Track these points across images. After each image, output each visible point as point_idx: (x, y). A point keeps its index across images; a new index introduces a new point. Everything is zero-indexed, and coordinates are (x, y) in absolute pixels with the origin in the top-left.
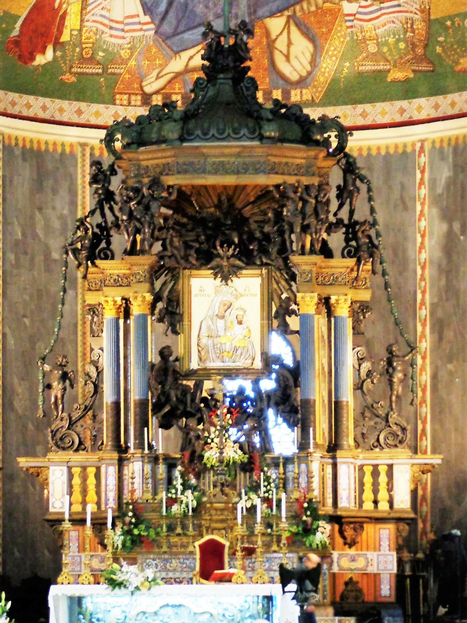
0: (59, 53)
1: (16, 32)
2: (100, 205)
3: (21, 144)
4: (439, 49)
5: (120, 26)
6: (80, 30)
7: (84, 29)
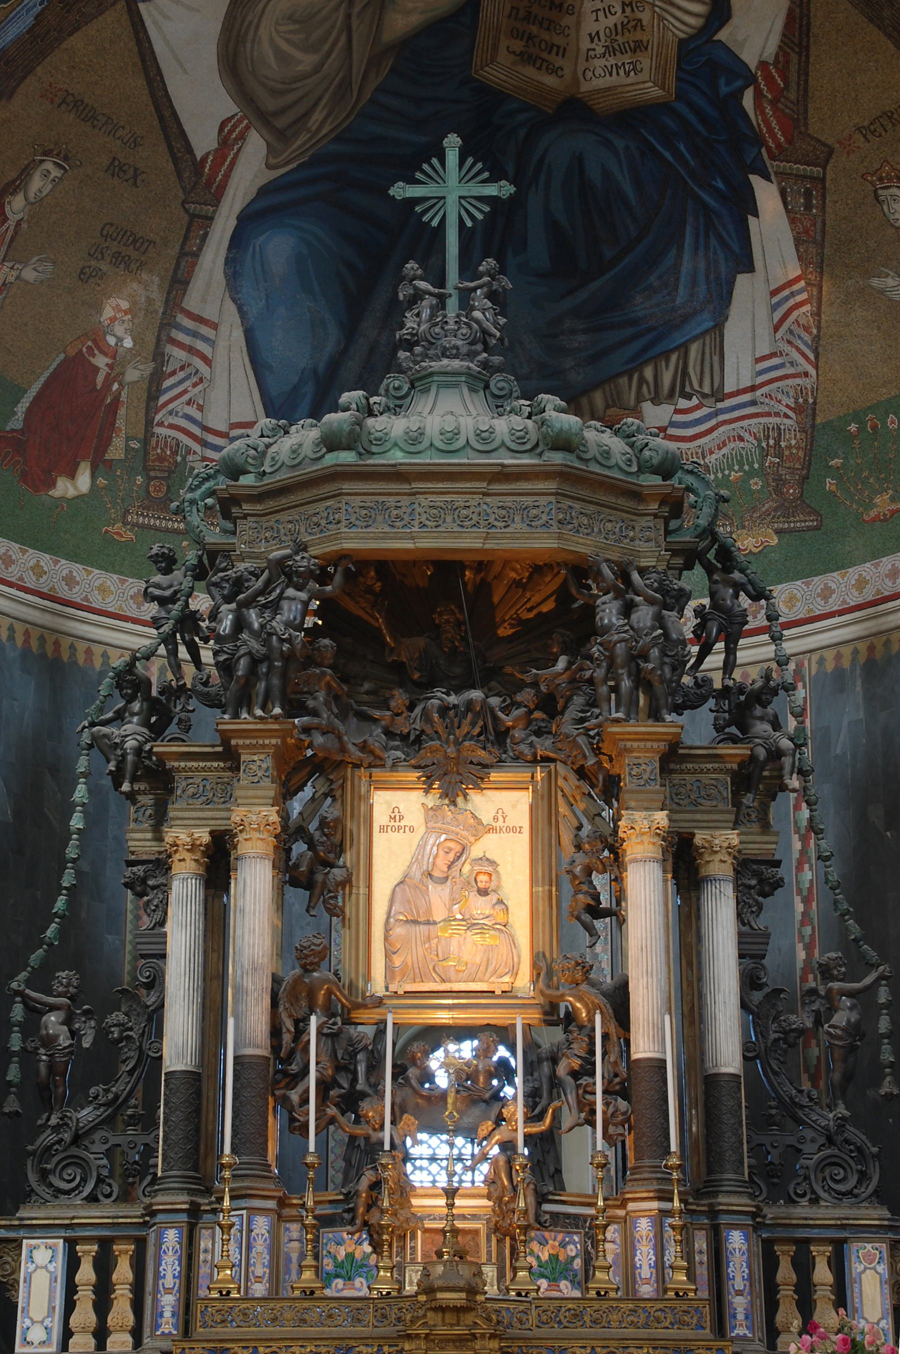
0: (101, 481)
6: (146, 442)
7: (153, 442)
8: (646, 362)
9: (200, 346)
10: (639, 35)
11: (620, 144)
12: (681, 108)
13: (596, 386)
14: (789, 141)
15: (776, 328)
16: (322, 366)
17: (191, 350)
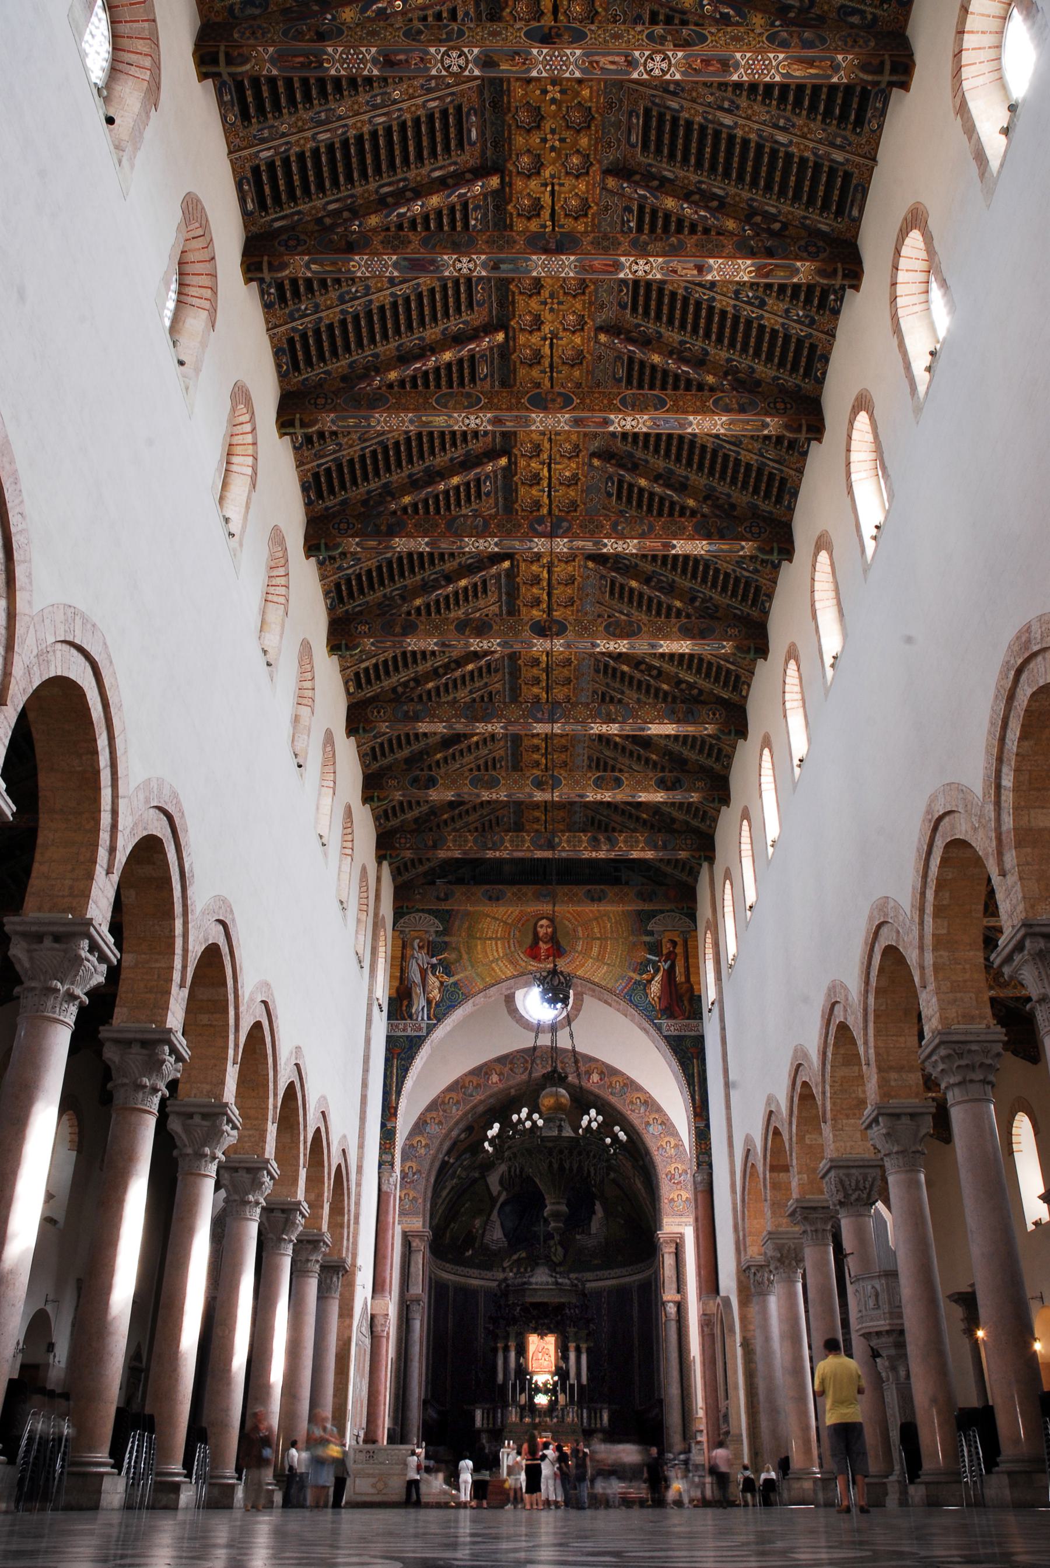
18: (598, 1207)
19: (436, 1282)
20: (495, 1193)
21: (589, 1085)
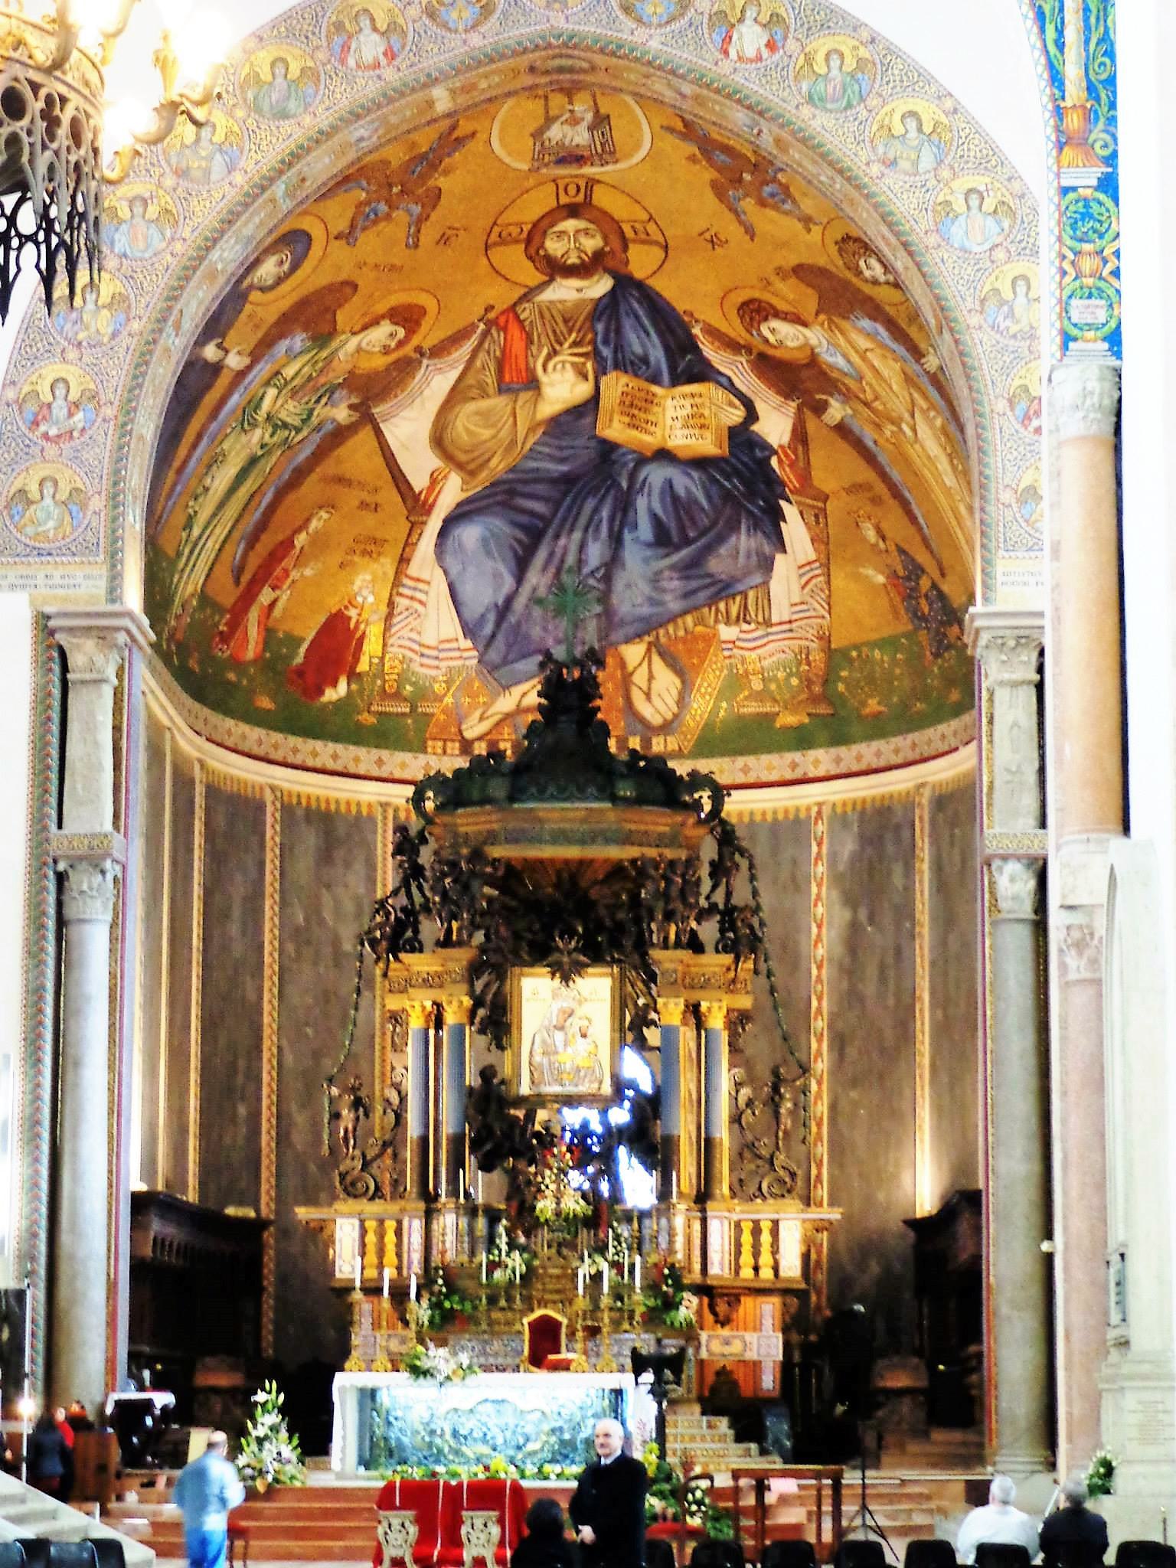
1: (299, 659)
2: (405, 883)
3: (304, 802)
4: (841, 687)
5: (434, 653)
6: (382, 659)
7: (387, 657)
8: (721, 599)
9: (419, 595)
10: (702, 421)
11: (695, 474)
12: (733, 461)
13: (685, 613)
14: (802, 486)
15: (803, 588)
16: (500, 602)
17: (412, 598)
18: (794, 526)
19: (212, 791)
20: (419, 482)
21: (726, 67)
